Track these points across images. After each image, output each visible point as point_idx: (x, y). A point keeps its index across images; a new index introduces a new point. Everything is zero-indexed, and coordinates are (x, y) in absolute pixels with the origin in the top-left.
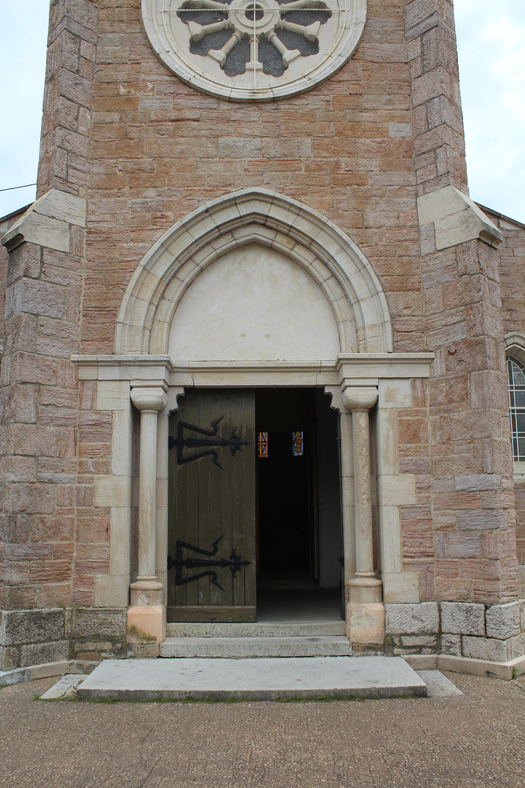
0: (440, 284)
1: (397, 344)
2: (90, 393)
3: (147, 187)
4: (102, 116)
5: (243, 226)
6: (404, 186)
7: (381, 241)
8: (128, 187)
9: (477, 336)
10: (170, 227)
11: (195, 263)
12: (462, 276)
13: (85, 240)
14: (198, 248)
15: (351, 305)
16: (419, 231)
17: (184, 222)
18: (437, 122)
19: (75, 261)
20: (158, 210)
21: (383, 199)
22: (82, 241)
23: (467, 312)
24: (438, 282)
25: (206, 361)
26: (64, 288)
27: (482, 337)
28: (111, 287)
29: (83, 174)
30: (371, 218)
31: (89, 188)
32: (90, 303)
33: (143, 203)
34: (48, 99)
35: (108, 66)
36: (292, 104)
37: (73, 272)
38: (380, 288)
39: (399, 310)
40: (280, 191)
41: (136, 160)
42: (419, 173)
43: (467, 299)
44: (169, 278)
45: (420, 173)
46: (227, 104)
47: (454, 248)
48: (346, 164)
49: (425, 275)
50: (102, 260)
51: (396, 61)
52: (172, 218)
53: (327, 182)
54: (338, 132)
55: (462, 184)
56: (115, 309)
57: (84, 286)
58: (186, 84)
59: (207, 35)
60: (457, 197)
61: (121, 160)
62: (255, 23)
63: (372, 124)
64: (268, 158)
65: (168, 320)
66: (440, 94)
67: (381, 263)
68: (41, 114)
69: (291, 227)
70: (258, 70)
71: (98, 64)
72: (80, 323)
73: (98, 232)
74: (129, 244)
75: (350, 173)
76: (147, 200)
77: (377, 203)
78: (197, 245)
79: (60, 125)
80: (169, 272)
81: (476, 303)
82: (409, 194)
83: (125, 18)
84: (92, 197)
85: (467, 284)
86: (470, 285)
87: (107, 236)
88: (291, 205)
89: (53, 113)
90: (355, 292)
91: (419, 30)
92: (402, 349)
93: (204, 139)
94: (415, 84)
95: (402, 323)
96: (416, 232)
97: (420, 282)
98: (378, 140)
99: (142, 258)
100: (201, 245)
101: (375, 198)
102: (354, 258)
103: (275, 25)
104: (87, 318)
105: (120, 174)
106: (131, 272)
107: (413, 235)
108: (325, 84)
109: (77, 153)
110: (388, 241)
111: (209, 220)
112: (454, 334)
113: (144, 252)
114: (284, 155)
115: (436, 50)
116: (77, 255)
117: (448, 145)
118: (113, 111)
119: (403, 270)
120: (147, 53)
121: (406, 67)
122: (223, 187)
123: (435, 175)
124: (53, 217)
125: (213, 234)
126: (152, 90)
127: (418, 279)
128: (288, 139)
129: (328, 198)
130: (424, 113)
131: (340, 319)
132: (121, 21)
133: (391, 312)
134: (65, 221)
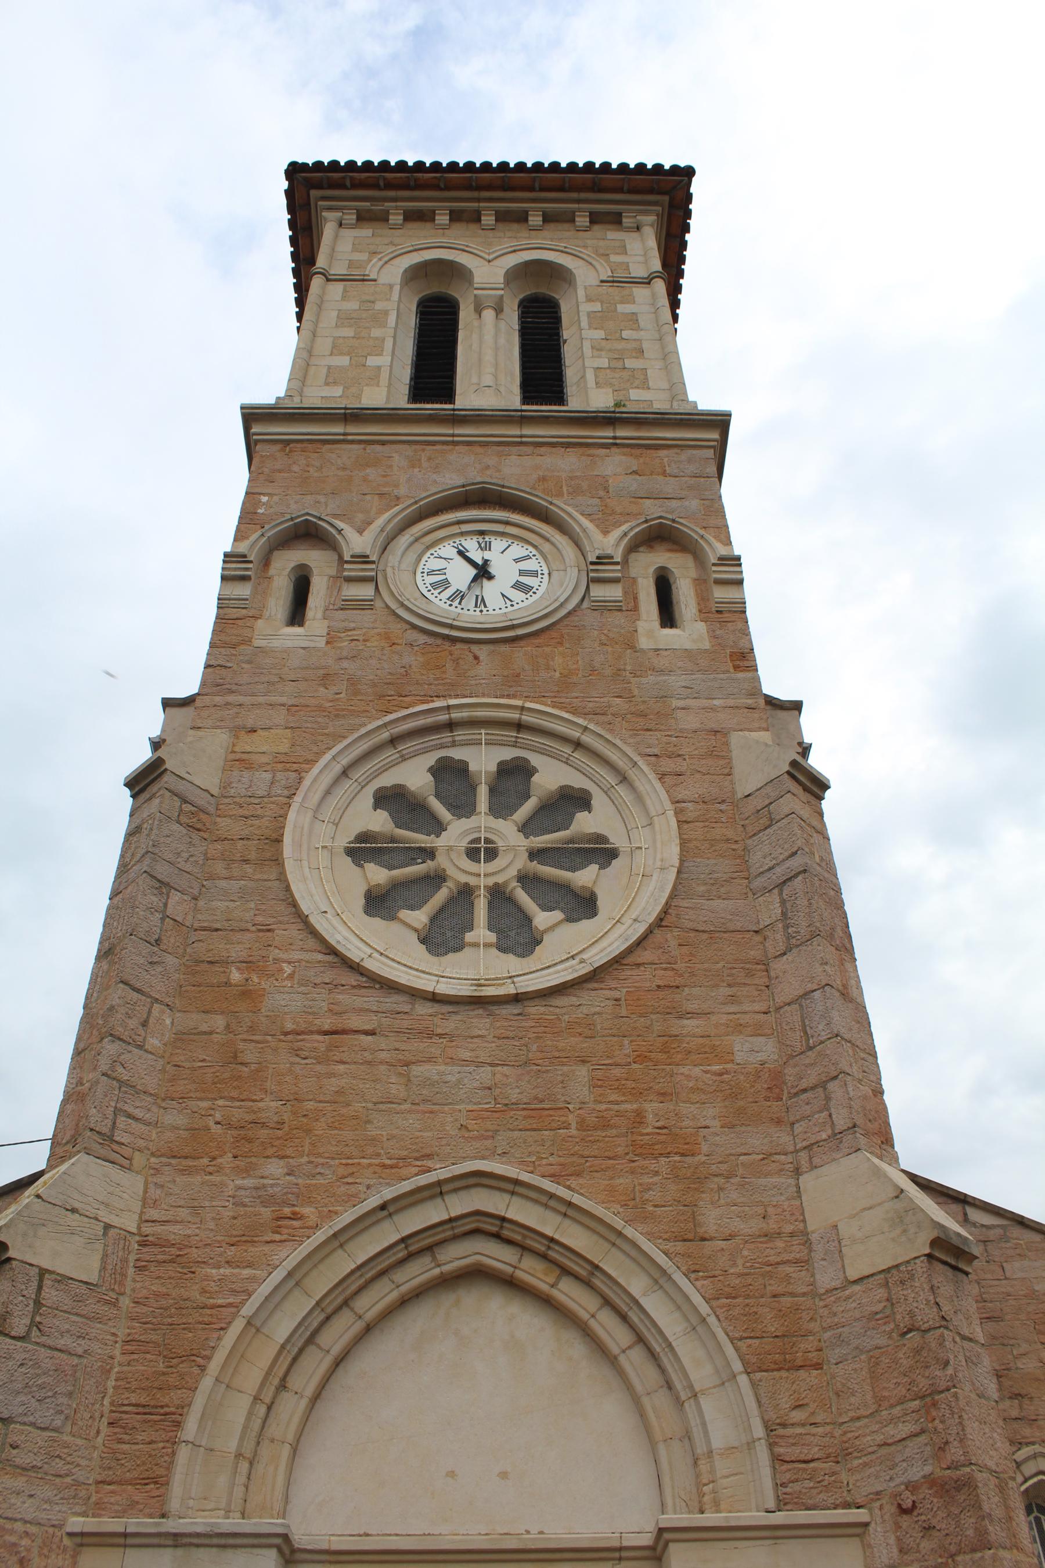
0: (862, 1352)
1: (784, 1490)
3: (267, 1157)
4: (194, 1020)
5: (455, 1238)
6: (771, 1154)
7: (735, 1265)
8: (230, 1155)
9: (956, 1468)
10: (309, 1237)
11: (355, 1313)
12: (906, 1333)
13: (132, 1258)
14: (362, 1281)
15: (679, 1404)
16: (807, 1243)
17: (336, 1228)
18: (823, 1033)
19: (107, 1302)
20: (285, 1203)
21: (732, 1180)
22: (125, 1261)
23: (928, 1412)
24: (857, 1348)
25: (367, 1535)
26: (76, 1361)
27: (968, 1470)
28: (175, 1361)
29: (143, 1127)
30: (711, 1219)
31: (153, 1154)
32: (127, 1395)
33: (256, 1188)
34: (98, 987)
35: (215, 933)
36: (551, 1006)
37: (99, 1326)
38: (737, 1366)
39: (781, 1412)
40: (530, 1169)
41: (251, 1103)
42: (798, 1128)
43: (923, 1384)
44: (300, 1344)
45: (801, 1129)
46: (429, 1004)
47: (882, 1276)
48: (657, 1114)
49: (829, 1334)
50: (163, 1302)
51: (739, 929)
52: (313, 1219)
53: (620, 1150)
54: (639, 1056)
55: (884, 1147)
56: (180, 1411)
57: (119, 1358)
58: (355, 968)
59: (396, 886)
60: (878, 1172)
61: (221, 1102)
62: (483, 868)
63: (701, 1040)
64: (506, 1105)
65: (290, 1437)
66: (823, 983)
67: (736, 1312)
68: (80, 1012)
69: (552, 1240)
70: (487, 945)
71: (196, 930)
72: (100, 1440)
73: (162, 1243)
74: (222, 1271)
75: (664, 1131)
76: (266, 1181)
77: (721, 1189)
78: (361, 1276)
79: (111, 1035)
80: (300, 1332)
81: (942, 1392)
82: (781, 1170)
83: (253, 856)
84: (157, 1171)
85: (917, 1351)
86: (924, 1353)
87: (178, 1253)
88: (552, 1196)
89: (101, 1012)
90: (686, 1376)
91: (774, 877)
92: (796, 1503)
93: (383, 1068)
94: (776, 966)
95: (791, 1441)
96: (804, 1245)
97: (820, 1350)
98: (716, 1068)
99: (247, 1300)
100: (369, 1275)
101: (716, 1179)
102: (681, 1303)
103: (519, 871)
104: (117, 1430)
105: (216, 1129)
106: (222, 1329)
107: (798, 1252)
108: (611, 969)
109: (138, 1087)
110: (748, 1264)
111: (386, 1225)
112: (905, 1464)
113: (250, 1289)
114: (536, 1098)
115: (807, 910)
116: (113, 1290)
117: (848, 1074)
118: (215, 1012)
119: (783, 1325)
120: (287, 913)
121: (758, 938)
122: (416, 1159)
123: (830, 1132)
124: (74, 1211)
125: (394, 1254)
126: (291, 976)
127: (816, 1343)
128: (544, 1068)
129: (623, 1182)
130: (797, 1018)
131: (658, 1436)
132: (245, 861)
133: (766, 1418)
134: (97, 1219)
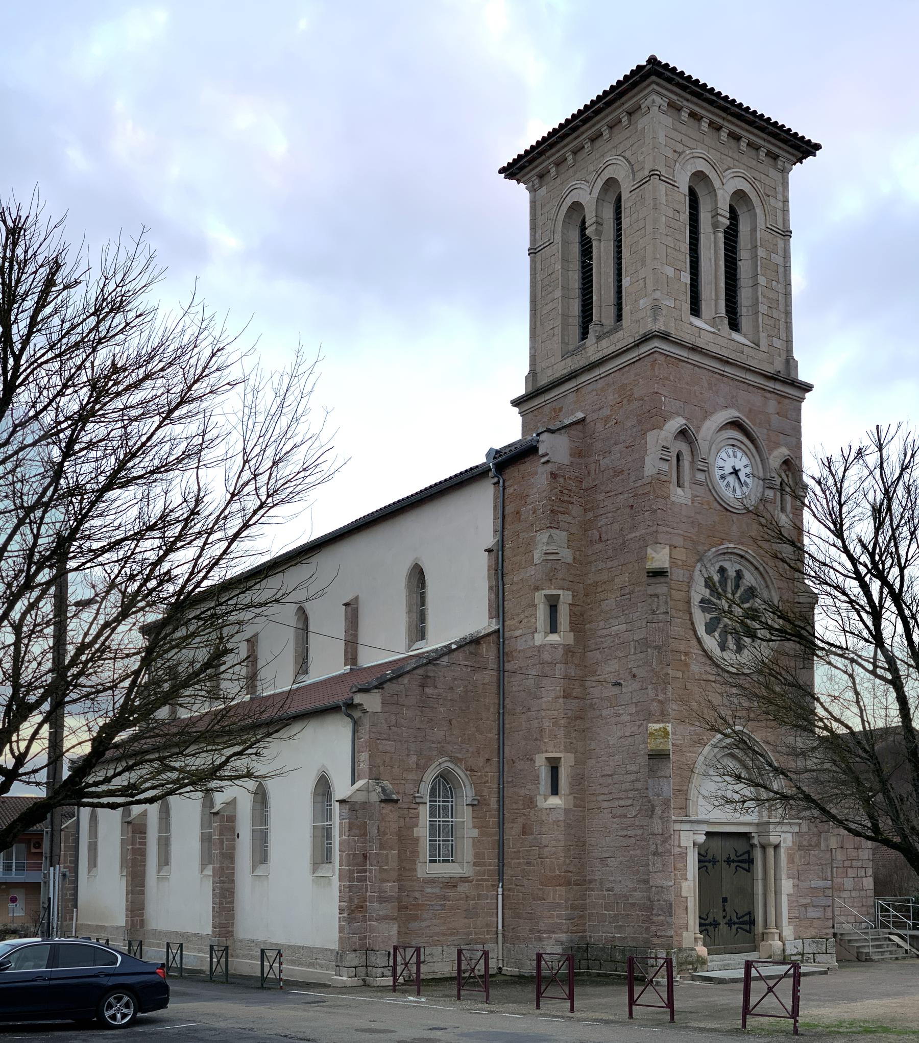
2: (677, 837)
